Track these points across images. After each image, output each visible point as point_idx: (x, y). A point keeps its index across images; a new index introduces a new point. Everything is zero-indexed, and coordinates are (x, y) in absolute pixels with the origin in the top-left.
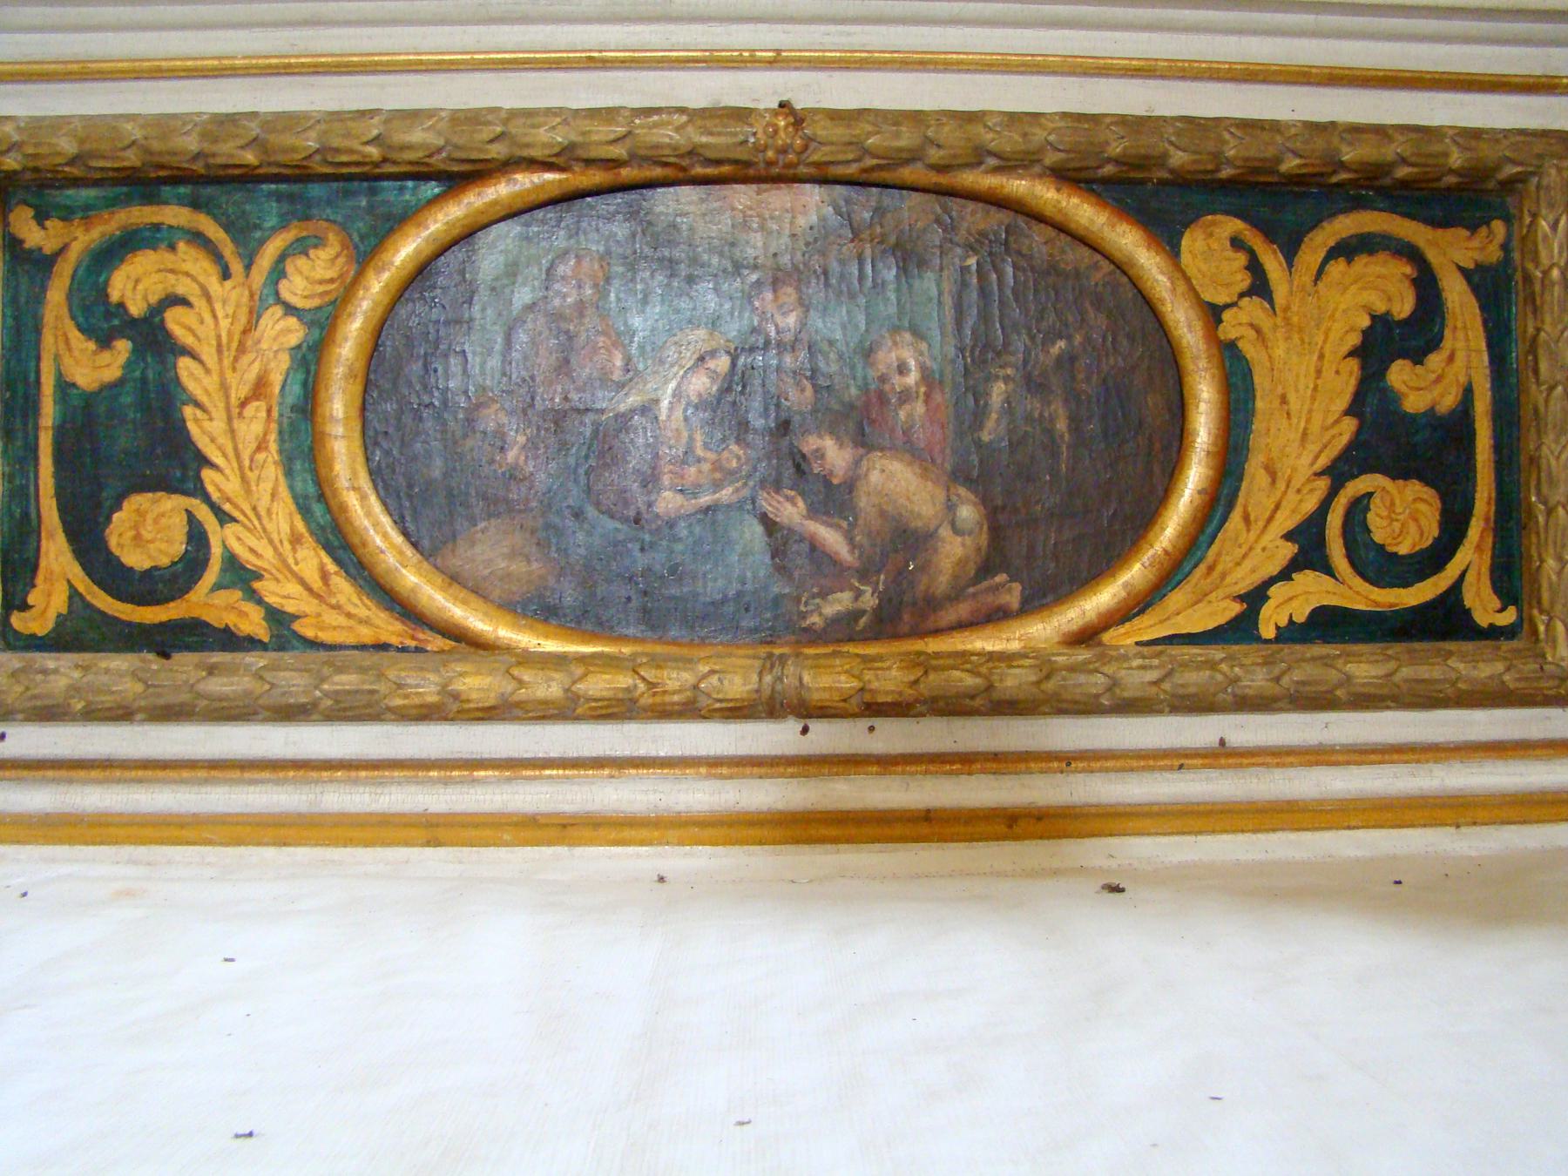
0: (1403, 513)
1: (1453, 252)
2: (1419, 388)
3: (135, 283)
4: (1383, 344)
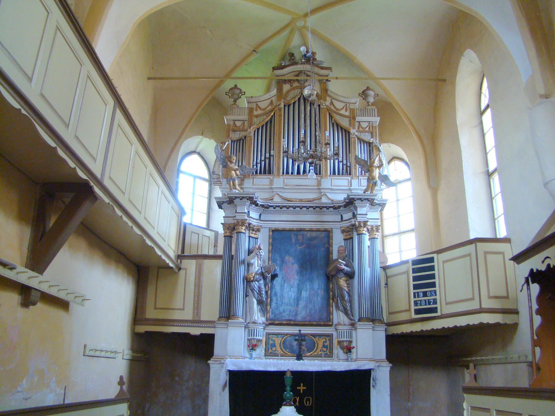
0: (325, 349)
1: (327, 338)
2: (326, 344)
3: (274, 339)
4: (324, 342)
